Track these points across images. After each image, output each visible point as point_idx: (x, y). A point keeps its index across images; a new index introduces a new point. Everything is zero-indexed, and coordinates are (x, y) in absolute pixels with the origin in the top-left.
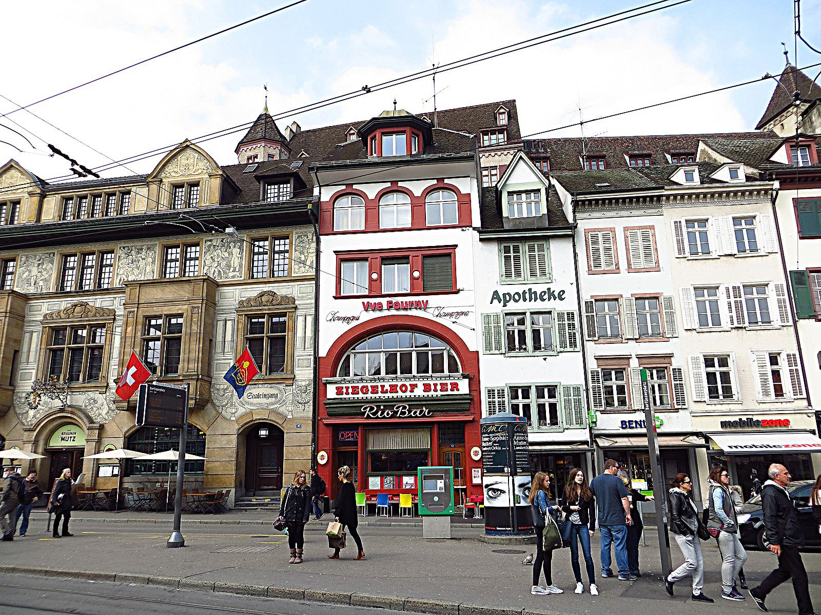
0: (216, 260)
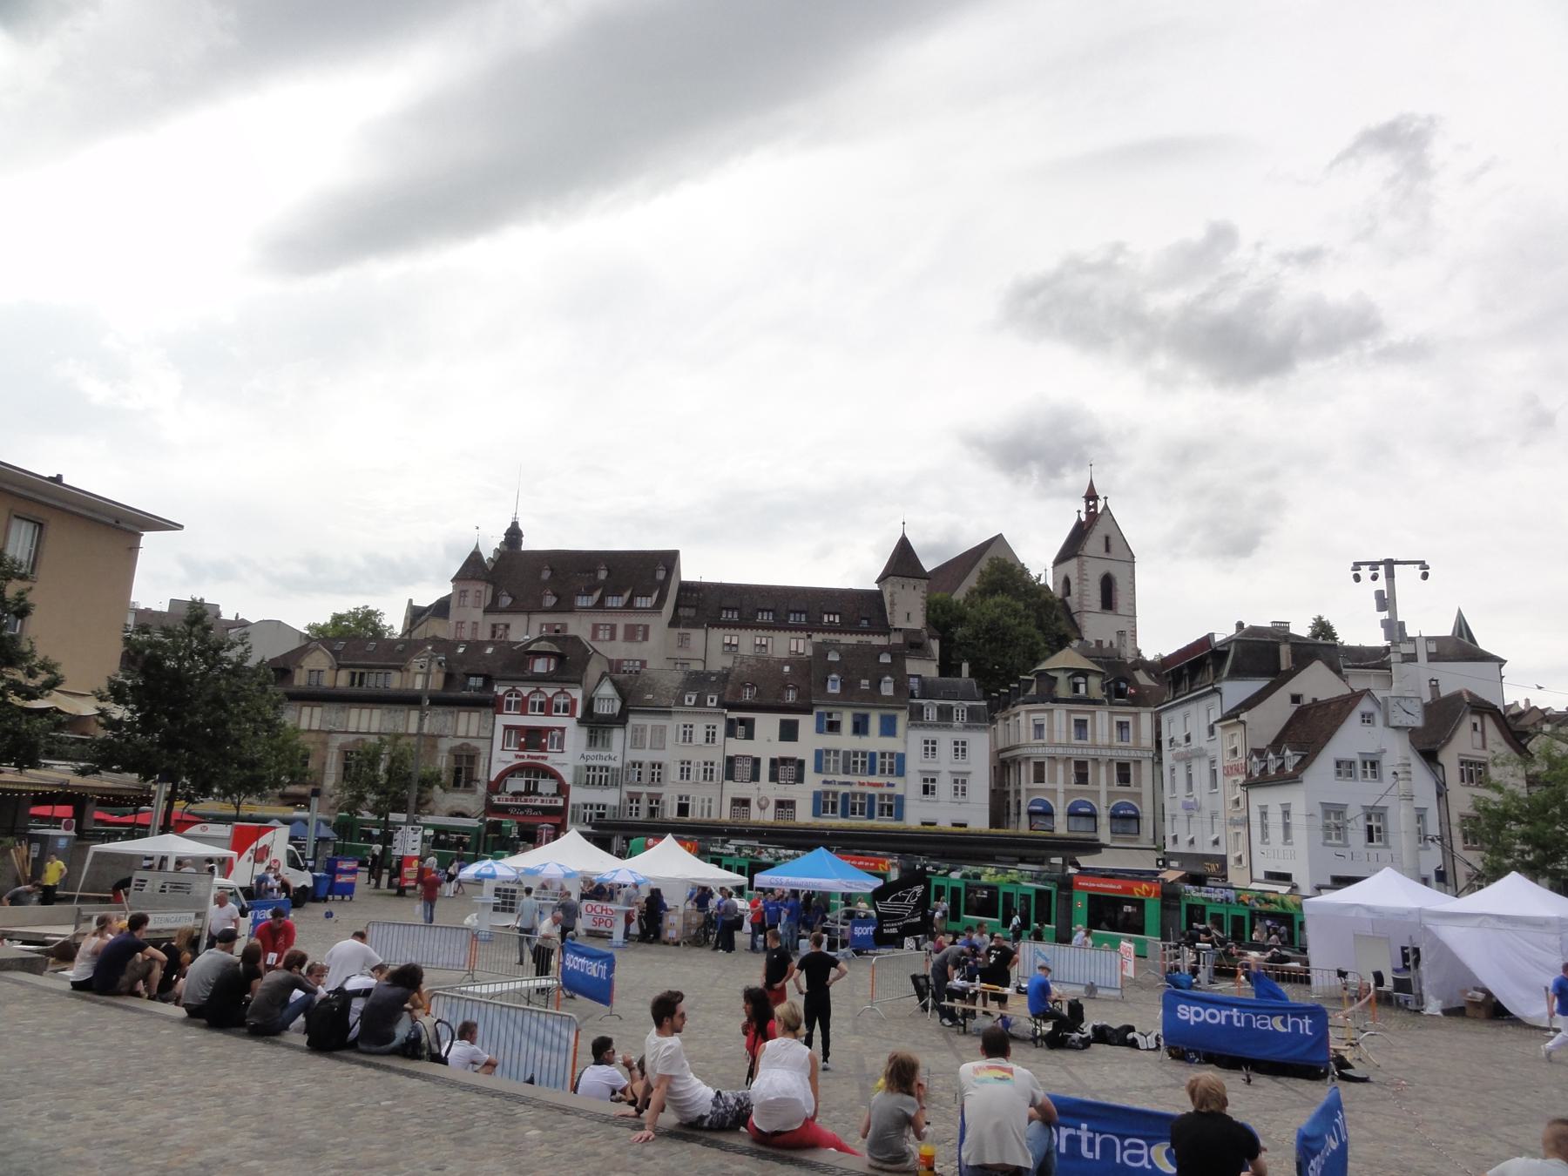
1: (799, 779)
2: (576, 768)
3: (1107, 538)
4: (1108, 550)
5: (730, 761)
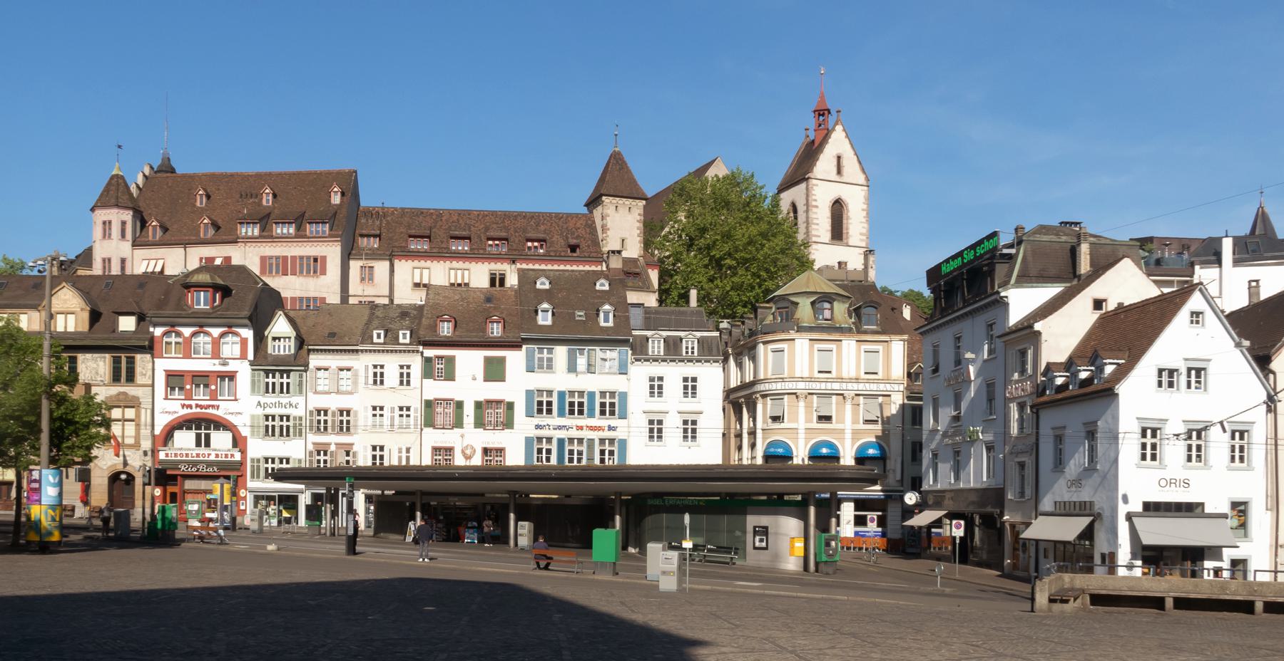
1: (508, 424)
2: (253, 417)
3: (839, 158)
4: (839, 172)
5: (429, 405)
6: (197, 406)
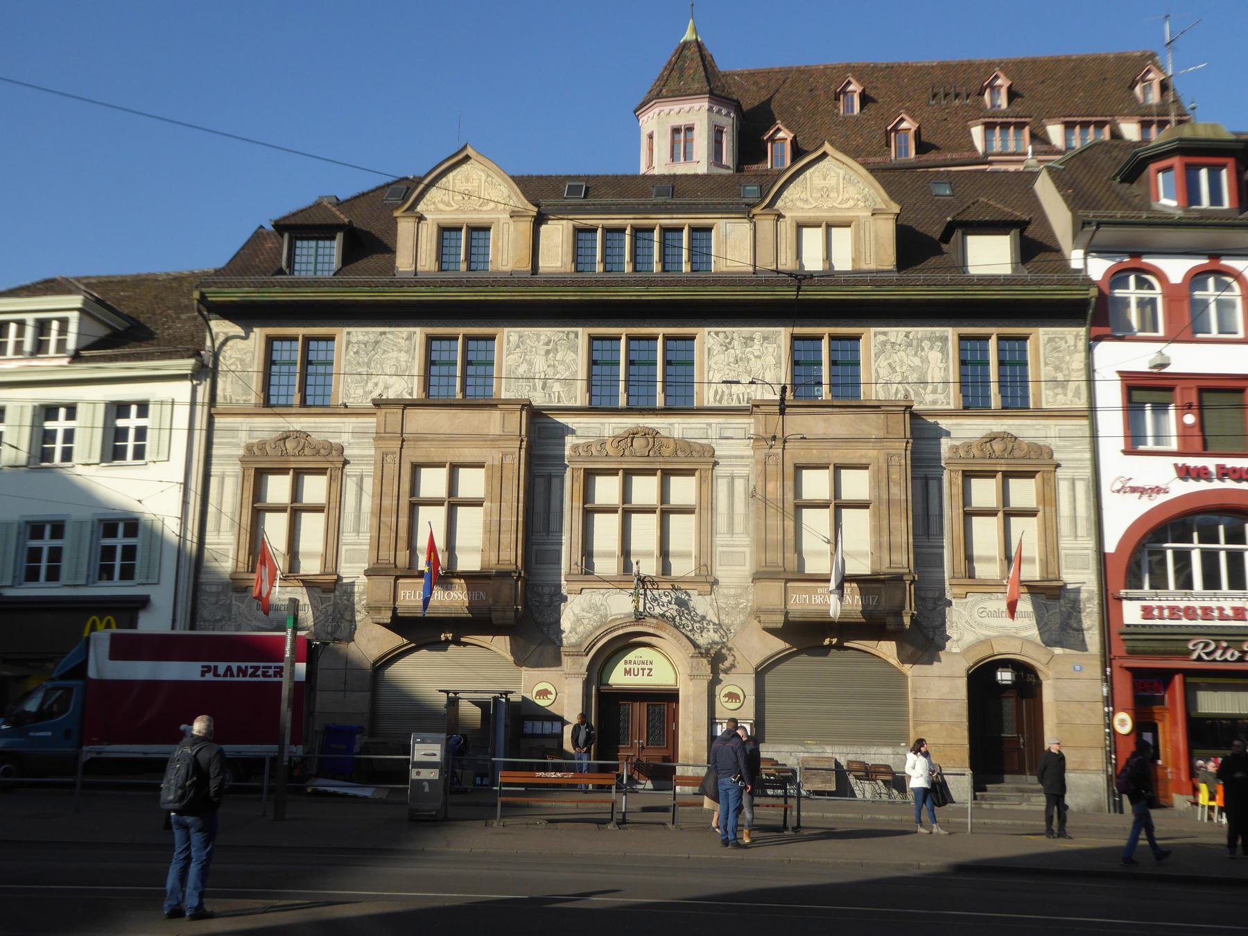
0: (898, 369)
6: (1223, 473)
